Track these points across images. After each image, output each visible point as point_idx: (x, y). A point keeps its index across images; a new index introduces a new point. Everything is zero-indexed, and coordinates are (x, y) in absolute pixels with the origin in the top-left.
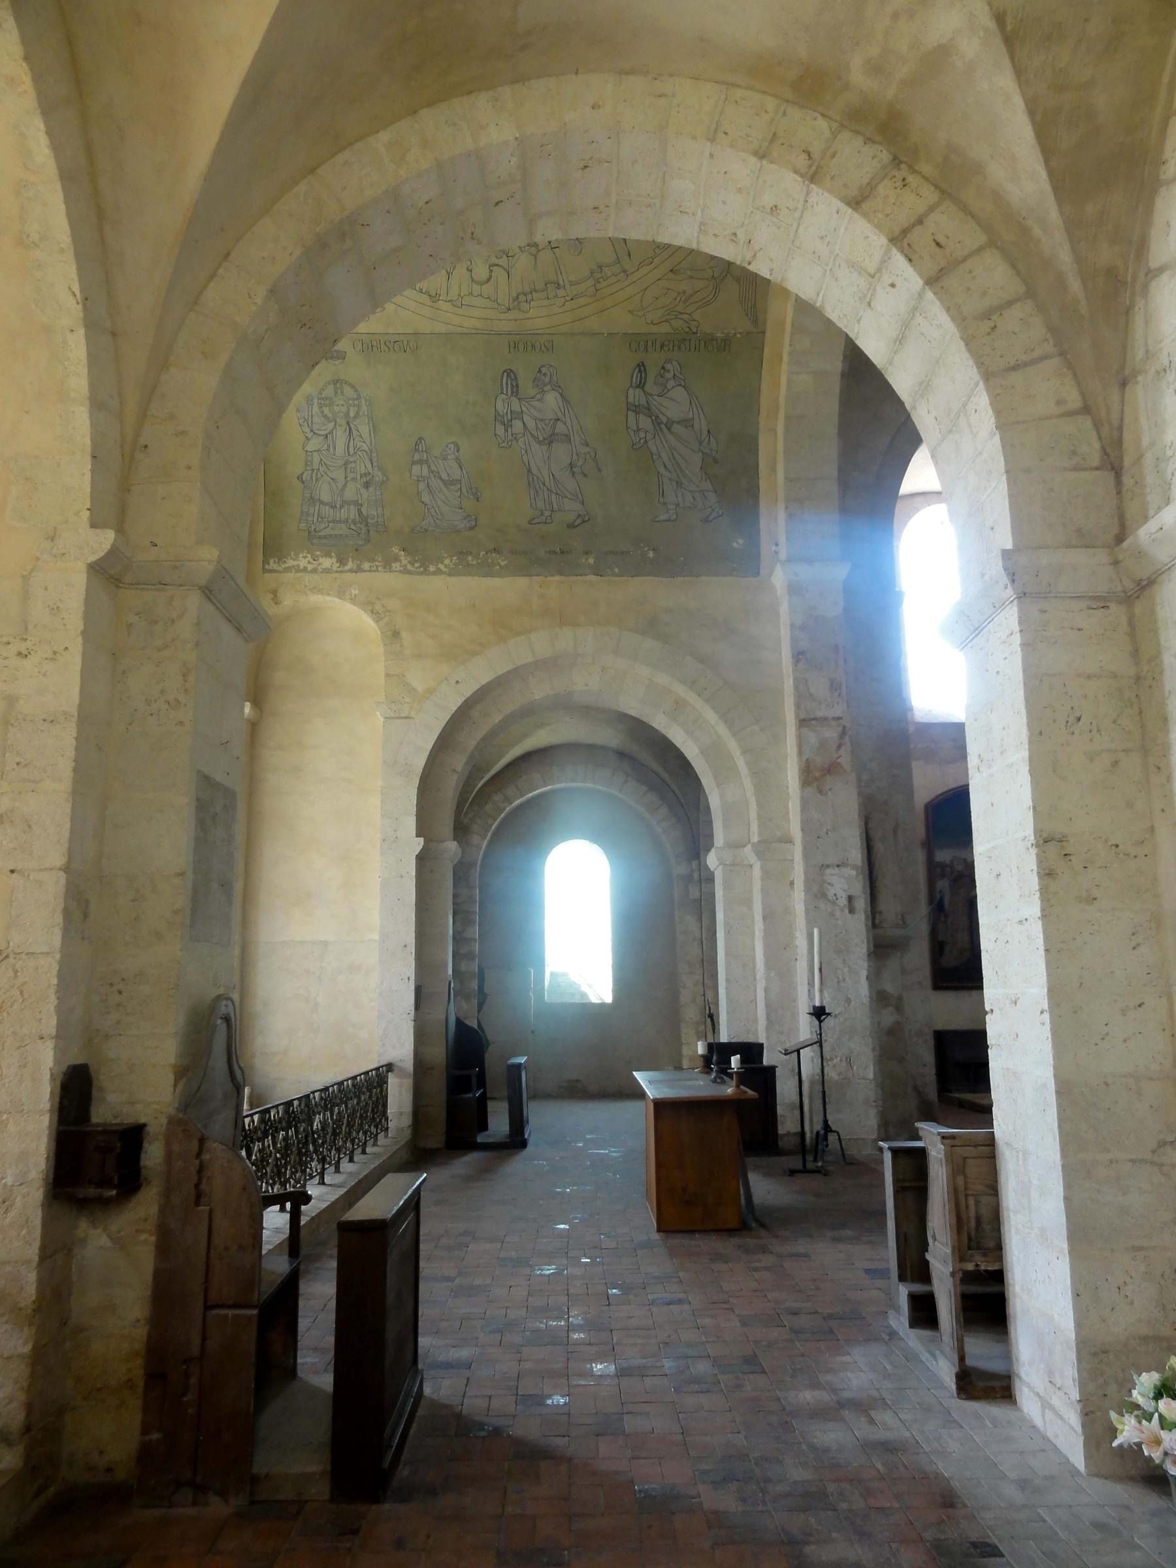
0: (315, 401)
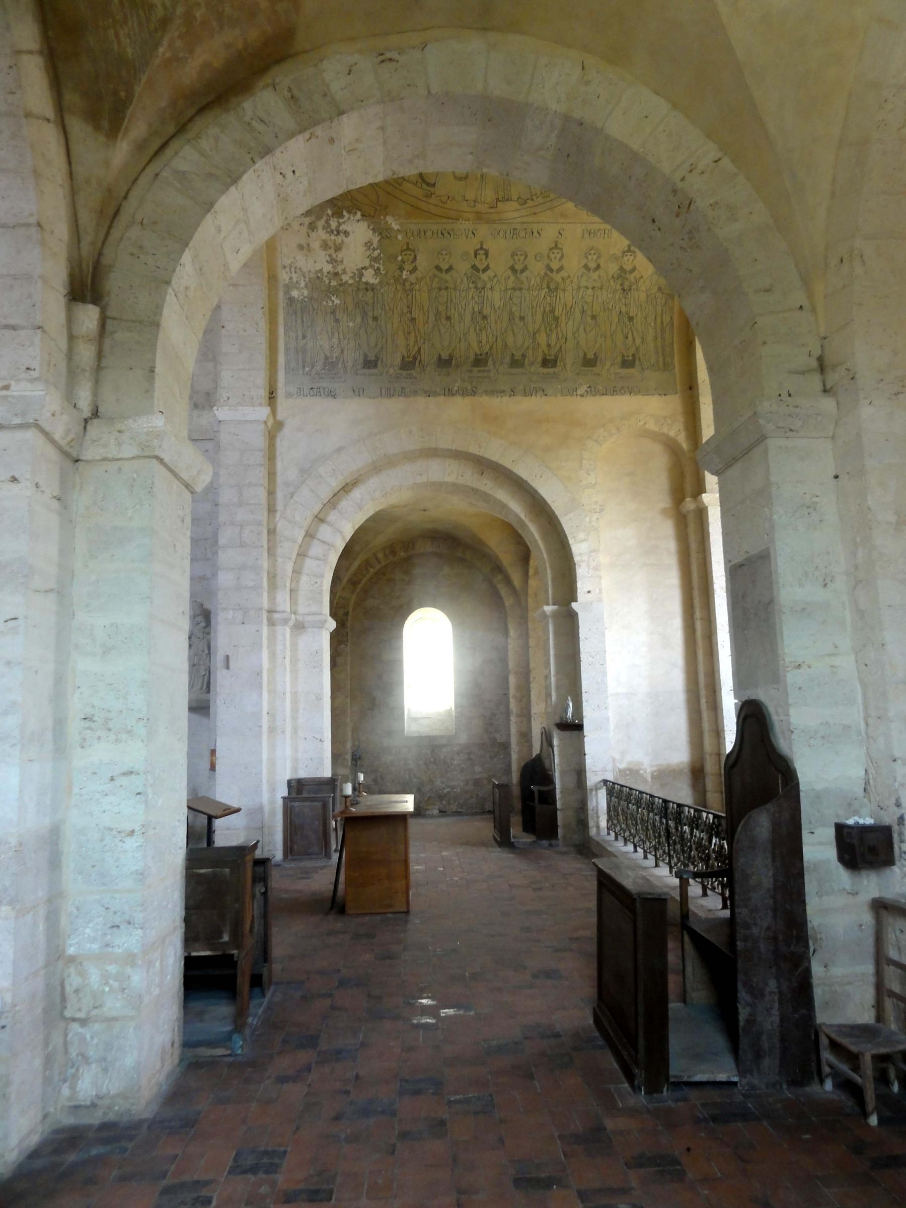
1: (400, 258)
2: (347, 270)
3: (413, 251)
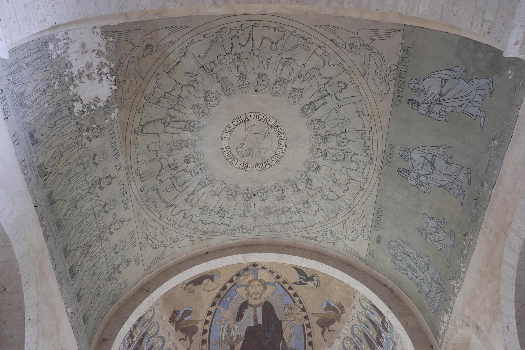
1: (94, 126)
2: (77, 88)
3: (101, 134)
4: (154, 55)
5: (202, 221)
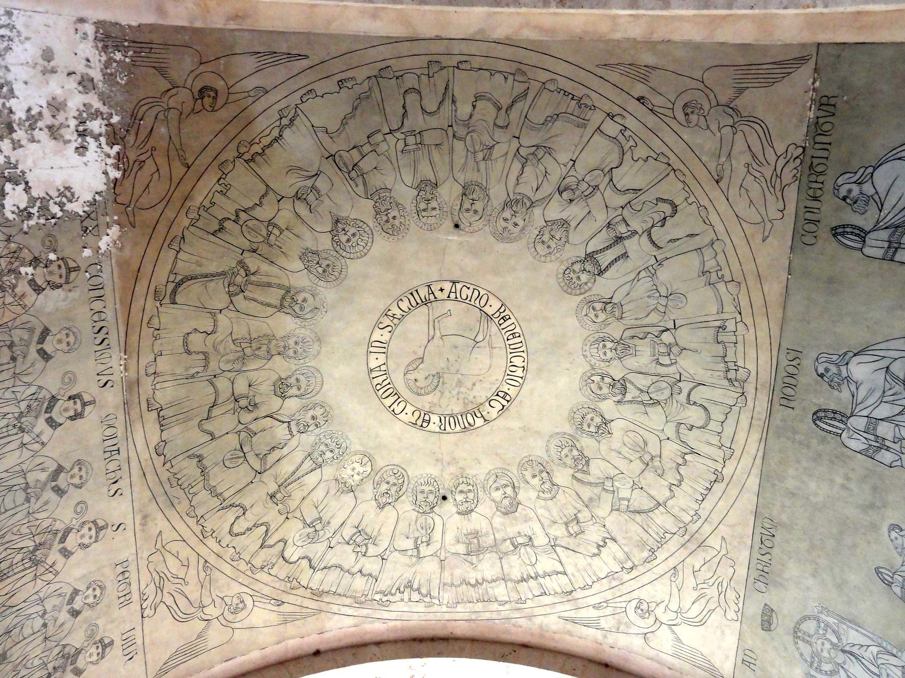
0: (813, 673)
1: (52, 256)
2: (20, 150)
4: (218, 114)
5: (310, 561)
